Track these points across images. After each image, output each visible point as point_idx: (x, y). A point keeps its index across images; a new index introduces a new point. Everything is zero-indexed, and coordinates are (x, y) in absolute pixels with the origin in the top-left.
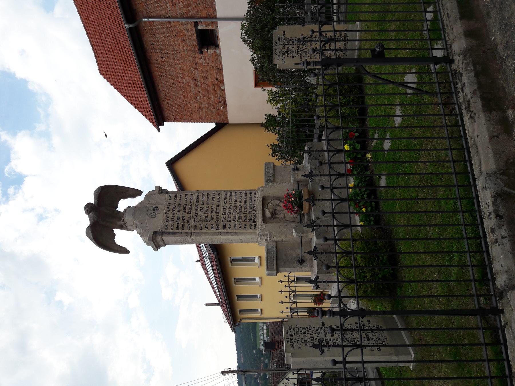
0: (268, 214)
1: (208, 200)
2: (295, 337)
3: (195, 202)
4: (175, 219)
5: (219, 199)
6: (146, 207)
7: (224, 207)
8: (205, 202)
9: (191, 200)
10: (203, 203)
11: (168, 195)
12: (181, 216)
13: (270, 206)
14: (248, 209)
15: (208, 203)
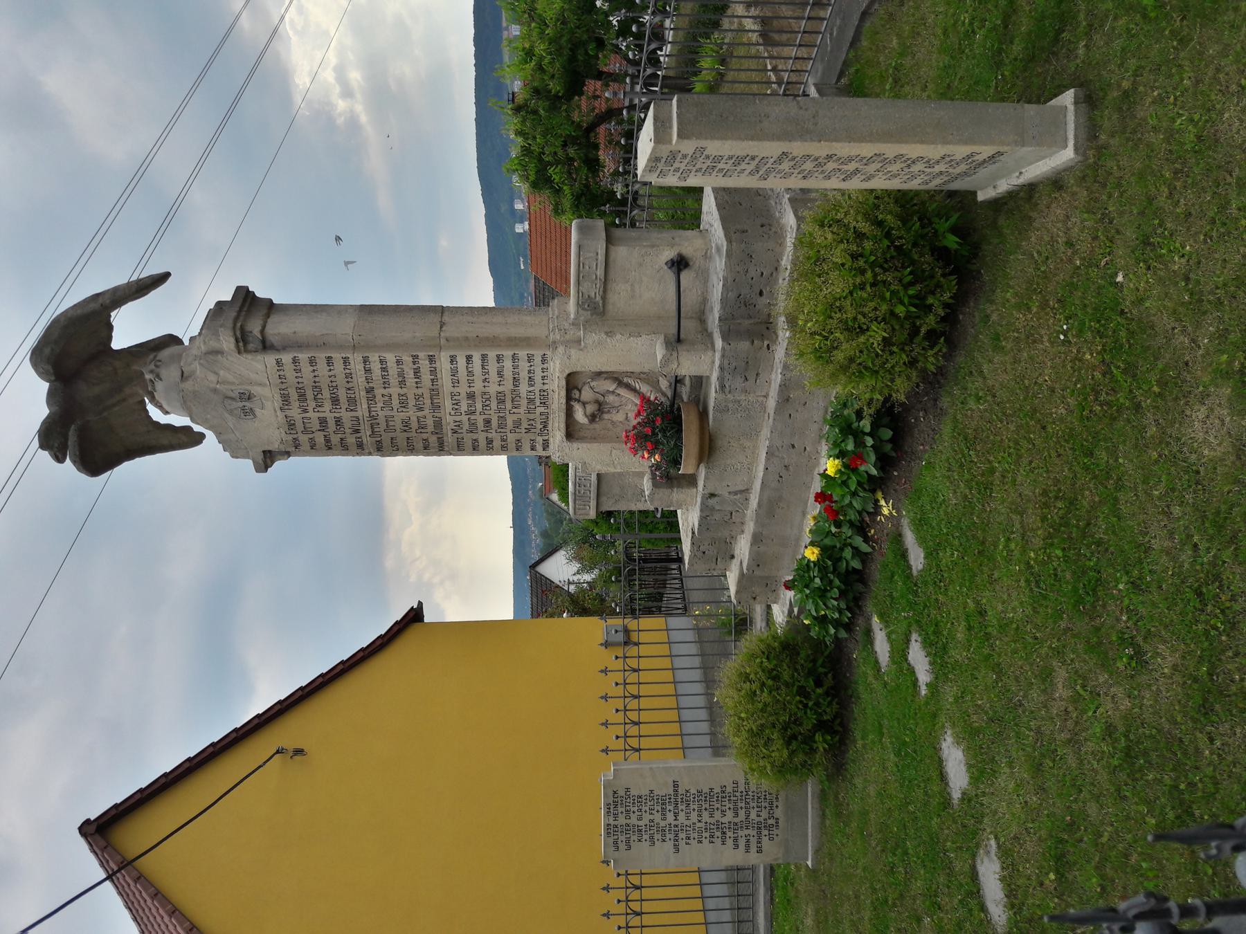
0: (580, 416)
1: (401, 374)
2: (622, 820)
3: (360, 380)
4: (316, 425)
5: (433, 372)
6: (215, 391)
7: (452, 395)
8: (394, 380)
9: (349, 376)
10: (386, 384)
11: (270, 359)
12: (331, 418)
13: (587, 394)
14: (524, 402)
15: (402, 383)
